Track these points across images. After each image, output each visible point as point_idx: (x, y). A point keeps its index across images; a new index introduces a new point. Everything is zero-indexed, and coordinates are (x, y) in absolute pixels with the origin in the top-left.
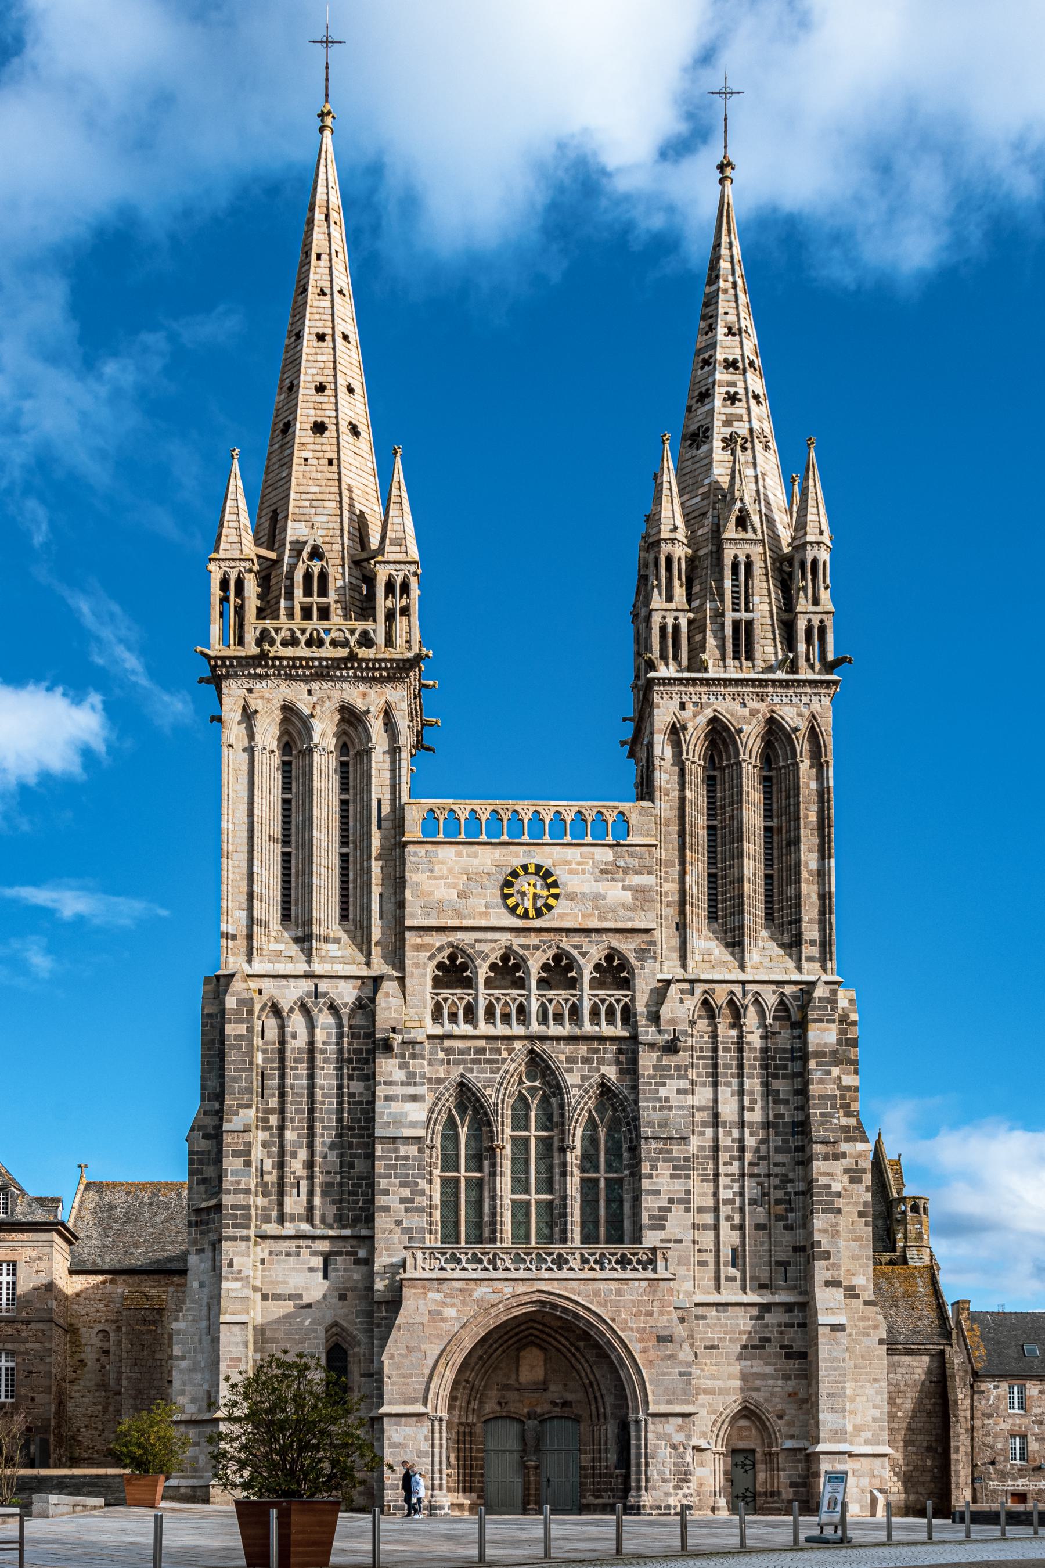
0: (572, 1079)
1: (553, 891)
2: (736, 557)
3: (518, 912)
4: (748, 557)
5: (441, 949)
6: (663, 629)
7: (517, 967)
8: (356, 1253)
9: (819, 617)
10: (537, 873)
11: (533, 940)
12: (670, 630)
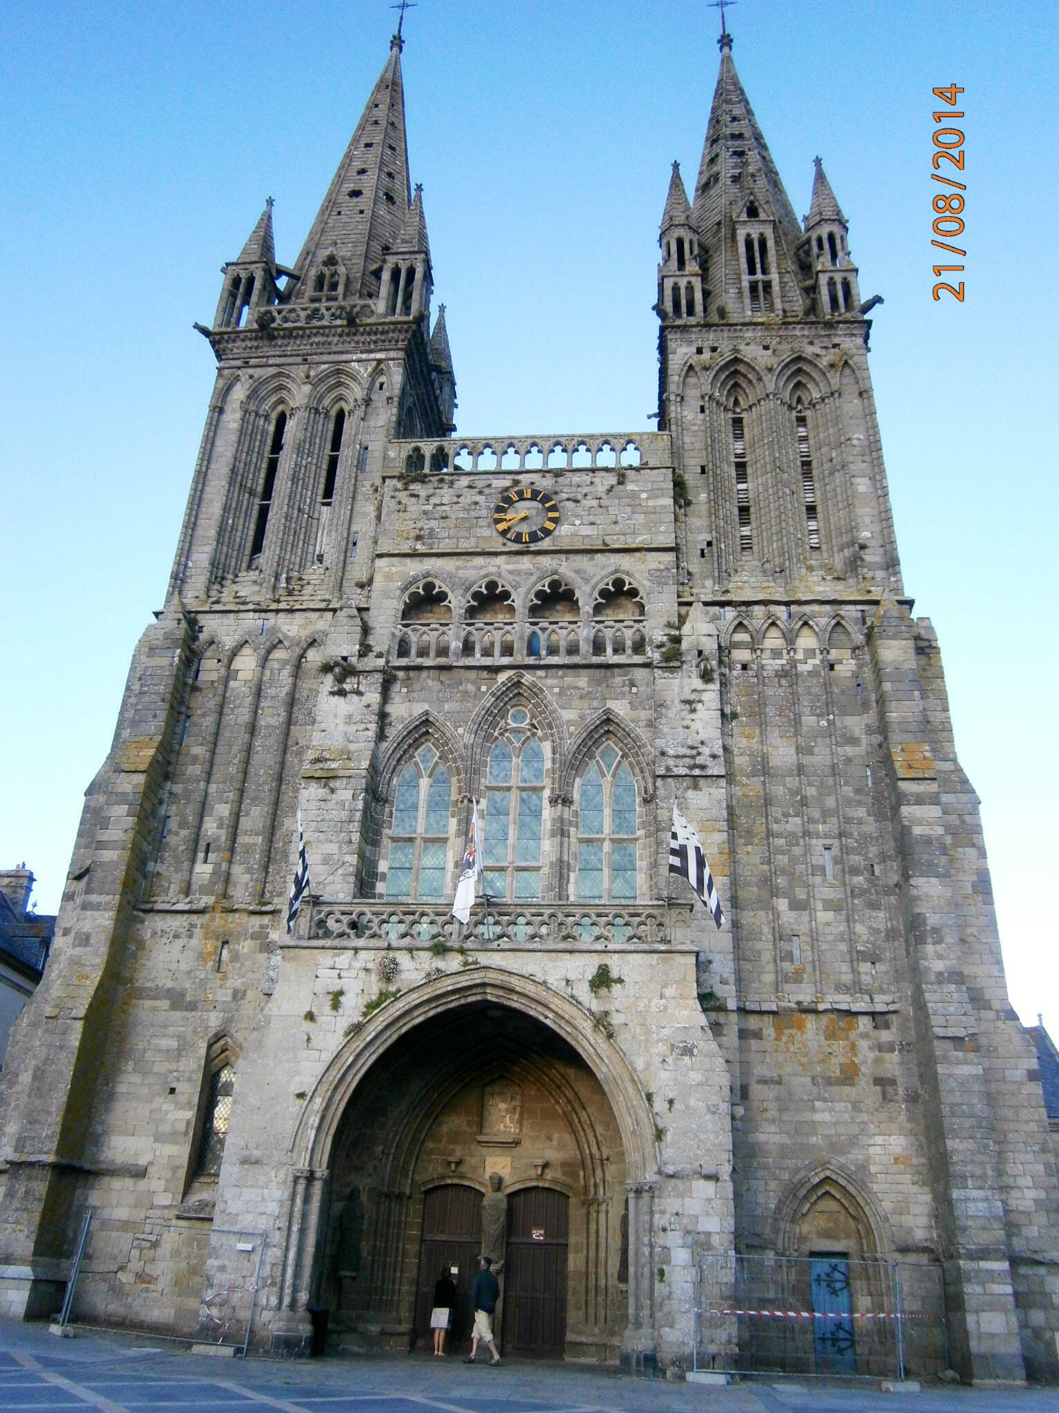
0: (568, 715)
1: (551, 515)
2: (748, 235)
3: (509, 536)
4: (762, 234)
5: (415, 580)
9: (843, 274)
10: (533, 498)
11: (526, 563)
12: (683, 291)
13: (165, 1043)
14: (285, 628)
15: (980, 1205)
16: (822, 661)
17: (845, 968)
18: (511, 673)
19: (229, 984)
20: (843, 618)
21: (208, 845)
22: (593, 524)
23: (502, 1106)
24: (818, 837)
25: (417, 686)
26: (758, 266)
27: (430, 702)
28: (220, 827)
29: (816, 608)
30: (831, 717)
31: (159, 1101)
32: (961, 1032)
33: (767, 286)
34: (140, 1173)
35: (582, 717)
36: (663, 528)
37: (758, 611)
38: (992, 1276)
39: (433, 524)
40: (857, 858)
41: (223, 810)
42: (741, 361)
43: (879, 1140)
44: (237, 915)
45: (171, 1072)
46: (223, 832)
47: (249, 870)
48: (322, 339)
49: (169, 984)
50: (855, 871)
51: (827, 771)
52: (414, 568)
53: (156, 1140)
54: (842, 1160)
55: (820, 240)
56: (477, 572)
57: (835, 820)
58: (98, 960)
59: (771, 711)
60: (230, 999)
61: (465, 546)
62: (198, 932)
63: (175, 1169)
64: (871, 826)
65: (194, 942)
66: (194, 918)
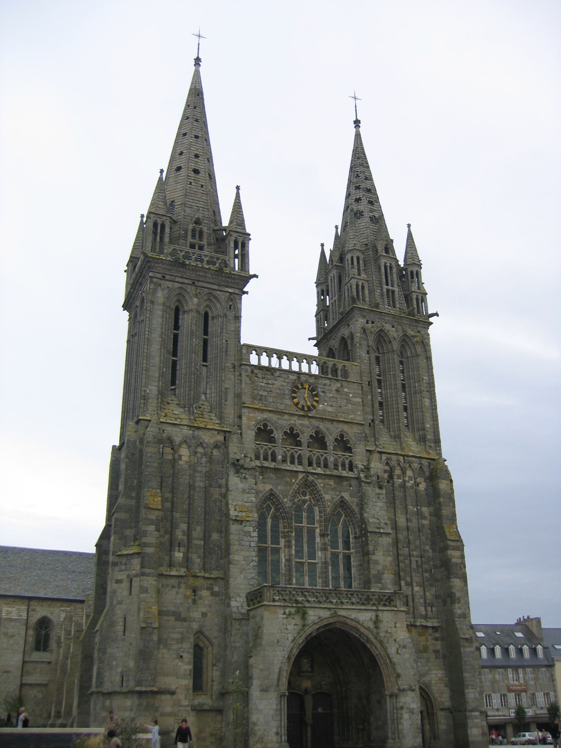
0: (327, 497)
2: (386, 263)
3: (299, 406)
4: (391, 264)
5: (260, 421)
6: (357, 286)
7: (297, 435)
8: (213, 589)
11: (306, 422)
12: (360, 287)
13: (176, 636)
14: (204, 437)
15: (473, 694)
16: (415, 482)
17: (423, 609)
18: (304, 475)
19: (199, 610)
20: (422, 464)
21: (179, 543)
22: (332, 406)
23: (305, 661)
24: (414, 556)
25: (266, 476)
26: (390, 282)
27: (272, 485)
28: (184, 535)
29: (413, 459)
30: (418, 507)
31: (177, 660)
32: (468, 637)
33: (393, 292)
34: (173, 693)
35: (333, 499)
36: (359, 413)
37: (394, 458)
38: (476, 717)
39: (265, 393)
40: (426, 566)
41: (184, 526)
42: (383, 331)
43: (434, 672)
44: (199, 579)
45: (180, 648)
46: (185, 538)
47: (199, 557)
48: (204, 274)
49: (173, 609)
50: (426, 572)
51: (417, 530)
52: (260, 416)
53: (177, 678)
54: (424, 679)
55: (412, 272)
56: (285, 422)
57: (419, 550)
58: (153, 600)
59: (398, 502)
60: (200, 616)
61: (281, 407)
62: (183, 586)
63: (188, 690)
64: (430, 553)
65: (181, 590)
66: (180, 579)
